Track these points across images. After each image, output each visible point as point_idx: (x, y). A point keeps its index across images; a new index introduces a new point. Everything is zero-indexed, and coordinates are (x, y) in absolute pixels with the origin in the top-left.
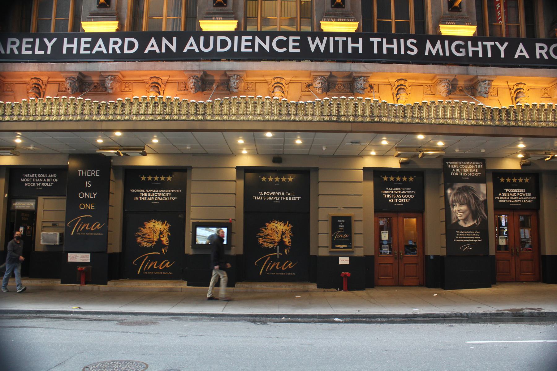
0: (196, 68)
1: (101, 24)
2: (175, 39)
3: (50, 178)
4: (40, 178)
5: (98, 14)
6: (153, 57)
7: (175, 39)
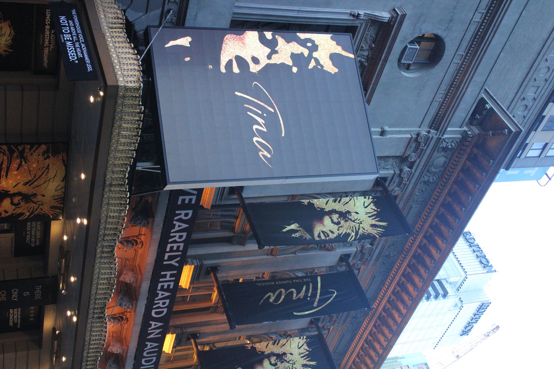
0: (129, 355)
1: (188, 277)
2: (160, 336)
3: (35, 240)
4: (36, 233)
5: (200, 270)
6: (145, 325)
7: (160, 336)
